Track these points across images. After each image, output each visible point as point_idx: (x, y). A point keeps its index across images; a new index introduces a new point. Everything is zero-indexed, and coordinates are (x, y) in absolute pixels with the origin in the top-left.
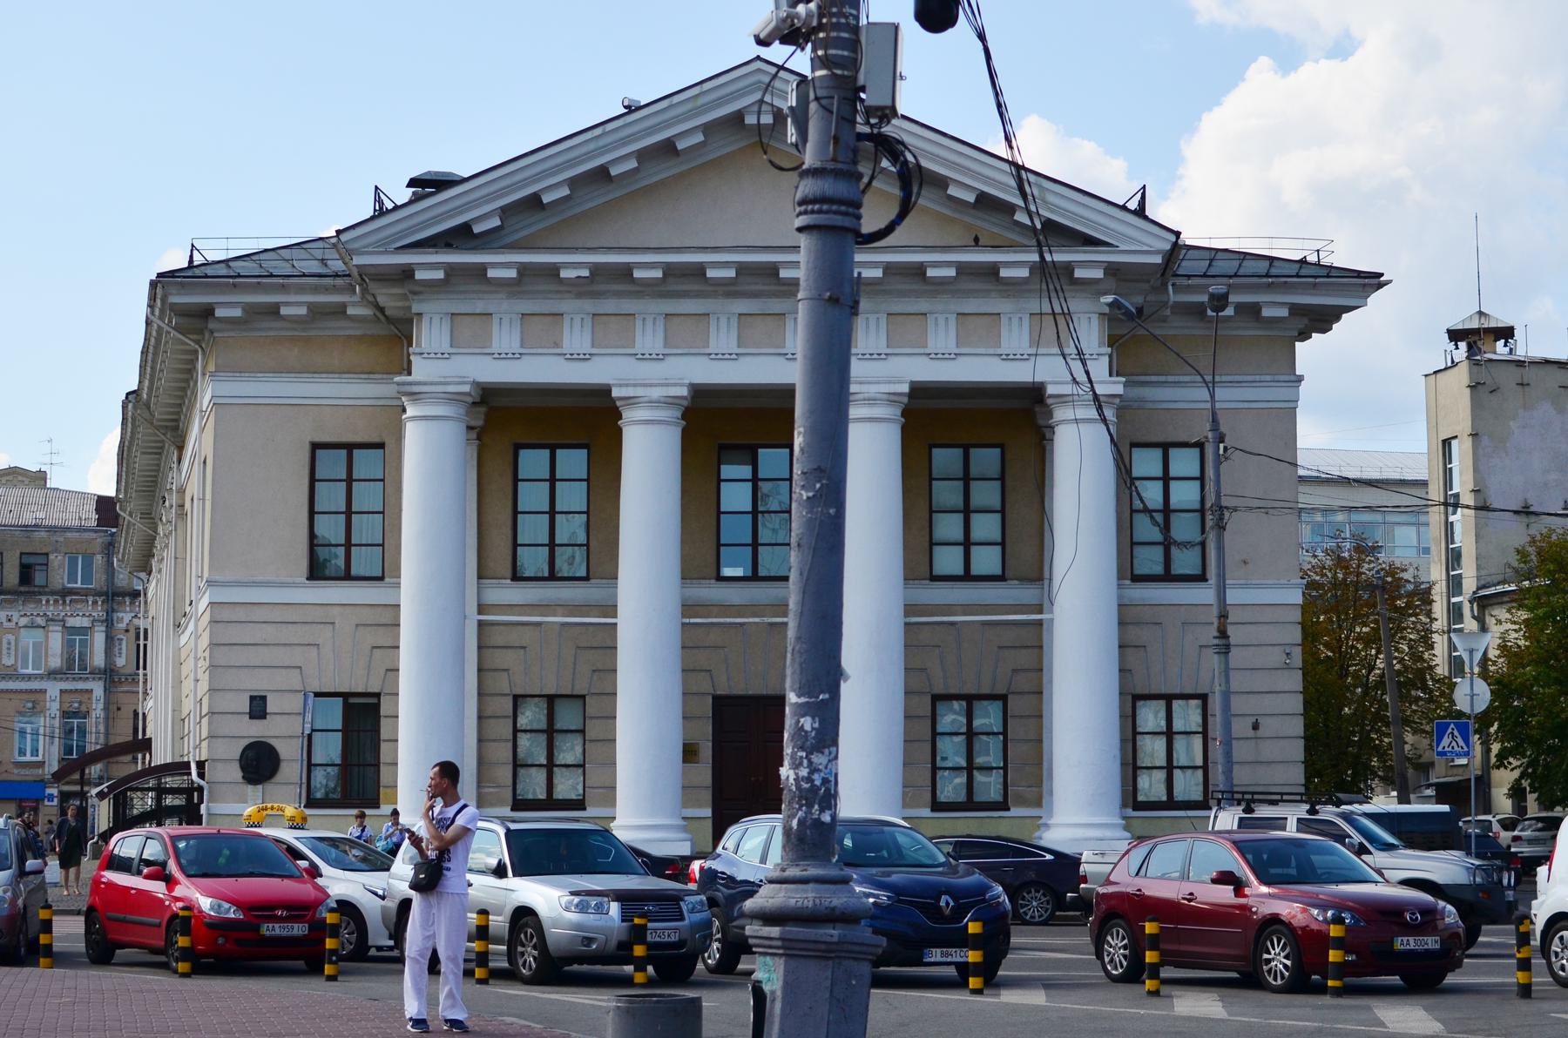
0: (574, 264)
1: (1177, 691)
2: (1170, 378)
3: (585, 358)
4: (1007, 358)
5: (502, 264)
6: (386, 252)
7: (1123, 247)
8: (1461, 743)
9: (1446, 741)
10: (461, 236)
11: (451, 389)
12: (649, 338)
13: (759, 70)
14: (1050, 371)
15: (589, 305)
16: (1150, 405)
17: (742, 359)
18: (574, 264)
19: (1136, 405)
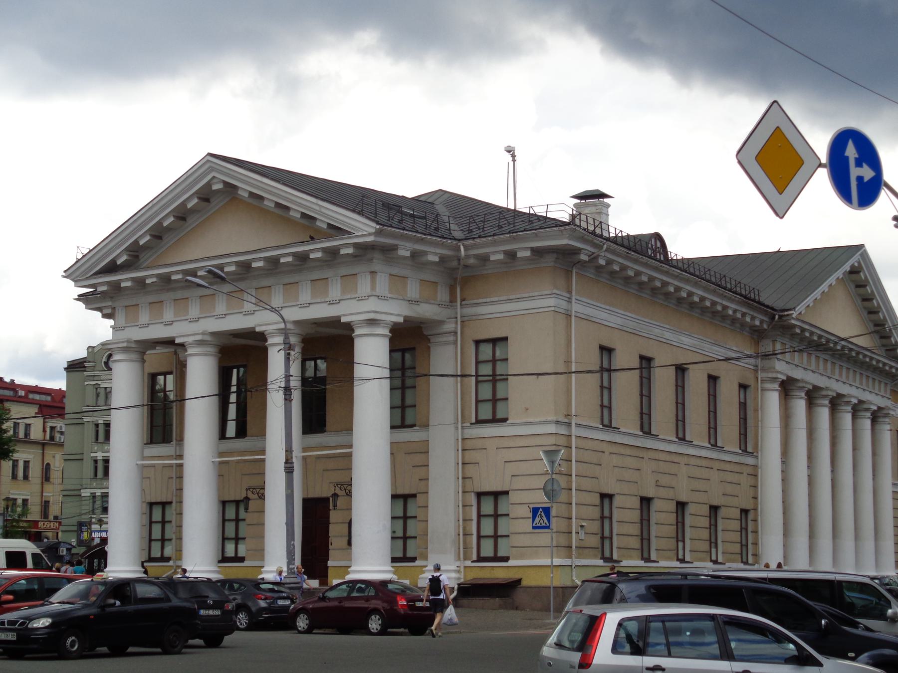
0: (150, 274)
1: (499, 489)
2: (488, 300)
3: (171, 323)
4: (331, 303)
5: (125, 279)
6: (88, 278)
7: (357, 234)
8: (546, 521)
9: (537, 519)
10: (112, 268)
11: (120, 345)
12: (194, 311)
13: (208, 161)
14: (350, 310)
15: (173, 295)
16: (481, 317)
17: (227, 317)
18: (150, 274)
19: (474, 318)
